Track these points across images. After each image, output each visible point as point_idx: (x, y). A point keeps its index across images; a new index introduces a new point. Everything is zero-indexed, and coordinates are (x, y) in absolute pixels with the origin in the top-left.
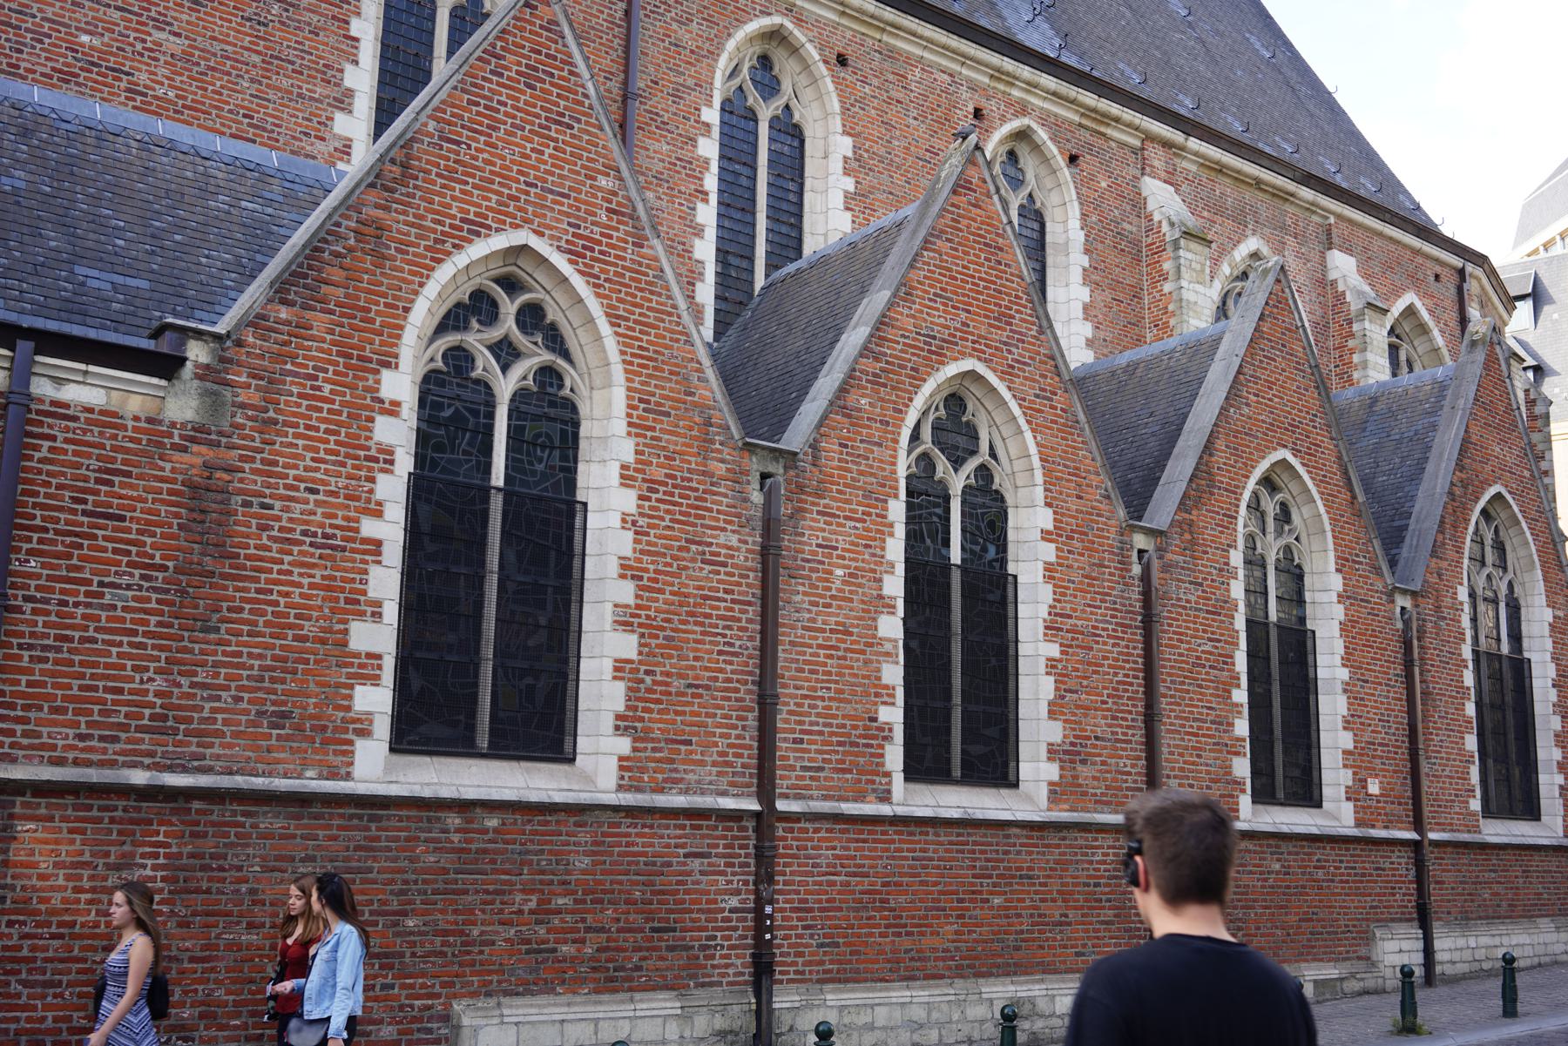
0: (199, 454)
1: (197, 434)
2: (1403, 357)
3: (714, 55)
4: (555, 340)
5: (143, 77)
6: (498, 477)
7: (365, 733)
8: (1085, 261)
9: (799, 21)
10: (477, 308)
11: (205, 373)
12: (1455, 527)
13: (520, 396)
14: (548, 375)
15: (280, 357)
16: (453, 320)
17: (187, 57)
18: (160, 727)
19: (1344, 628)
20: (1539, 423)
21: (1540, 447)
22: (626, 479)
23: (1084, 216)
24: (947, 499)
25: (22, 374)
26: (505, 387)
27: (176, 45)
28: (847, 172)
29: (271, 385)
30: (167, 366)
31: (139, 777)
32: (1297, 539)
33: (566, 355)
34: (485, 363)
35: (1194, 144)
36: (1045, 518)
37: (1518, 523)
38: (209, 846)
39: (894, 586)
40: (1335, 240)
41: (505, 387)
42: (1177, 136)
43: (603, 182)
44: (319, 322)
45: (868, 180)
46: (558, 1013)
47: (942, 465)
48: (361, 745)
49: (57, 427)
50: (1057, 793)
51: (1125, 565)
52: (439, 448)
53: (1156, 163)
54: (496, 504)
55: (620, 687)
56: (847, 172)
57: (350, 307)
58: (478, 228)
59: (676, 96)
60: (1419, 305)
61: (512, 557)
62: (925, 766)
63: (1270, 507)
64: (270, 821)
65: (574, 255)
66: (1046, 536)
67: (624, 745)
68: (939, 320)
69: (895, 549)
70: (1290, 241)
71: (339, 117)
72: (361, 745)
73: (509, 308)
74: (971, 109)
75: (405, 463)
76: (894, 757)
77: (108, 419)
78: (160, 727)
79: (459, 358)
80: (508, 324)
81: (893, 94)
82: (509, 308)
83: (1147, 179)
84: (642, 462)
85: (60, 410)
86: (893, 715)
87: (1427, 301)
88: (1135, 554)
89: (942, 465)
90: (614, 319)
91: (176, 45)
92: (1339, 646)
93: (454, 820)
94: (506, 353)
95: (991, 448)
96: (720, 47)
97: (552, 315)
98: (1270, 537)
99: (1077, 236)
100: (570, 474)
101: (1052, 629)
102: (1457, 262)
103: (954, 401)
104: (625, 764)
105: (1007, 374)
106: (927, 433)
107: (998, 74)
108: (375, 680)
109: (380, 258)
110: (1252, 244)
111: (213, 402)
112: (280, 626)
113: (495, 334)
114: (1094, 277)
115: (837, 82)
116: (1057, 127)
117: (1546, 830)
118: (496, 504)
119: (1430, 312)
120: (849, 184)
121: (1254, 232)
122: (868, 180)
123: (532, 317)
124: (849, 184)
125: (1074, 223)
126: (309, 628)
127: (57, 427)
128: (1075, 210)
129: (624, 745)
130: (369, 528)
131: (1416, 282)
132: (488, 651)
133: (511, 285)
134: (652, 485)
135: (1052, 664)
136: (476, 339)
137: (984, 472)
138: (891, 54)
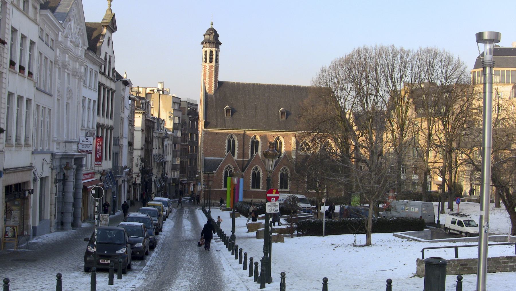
4: (231, 169)
10: (228, 168)
13: (229, 172)
14: (231, 170)
16: (226, 169)
26: (229, 172)
27: (216, 148)
34: (228, 170)
36: (262, 174)
39: (251, 179)
41: (229, 172)
47: (255, 171)
50: (262, 189)
58: (227, 165)
62: (253, 187)
69: (251, 177)
73: (229, 168)
75: (224, 176)
76: (251, 187)
79: (226, 170)
80: (229, 168)
82: (229, 168)
86: (251, 185)
89: (255, 171)
91: (216, 148)
94: (229, 170)
103: (256, 167)
107: (276, 133)
116: (282, 135)
123: (230, 168)
133: (229, 166)
136: (227, 169)
137: (258, 171)
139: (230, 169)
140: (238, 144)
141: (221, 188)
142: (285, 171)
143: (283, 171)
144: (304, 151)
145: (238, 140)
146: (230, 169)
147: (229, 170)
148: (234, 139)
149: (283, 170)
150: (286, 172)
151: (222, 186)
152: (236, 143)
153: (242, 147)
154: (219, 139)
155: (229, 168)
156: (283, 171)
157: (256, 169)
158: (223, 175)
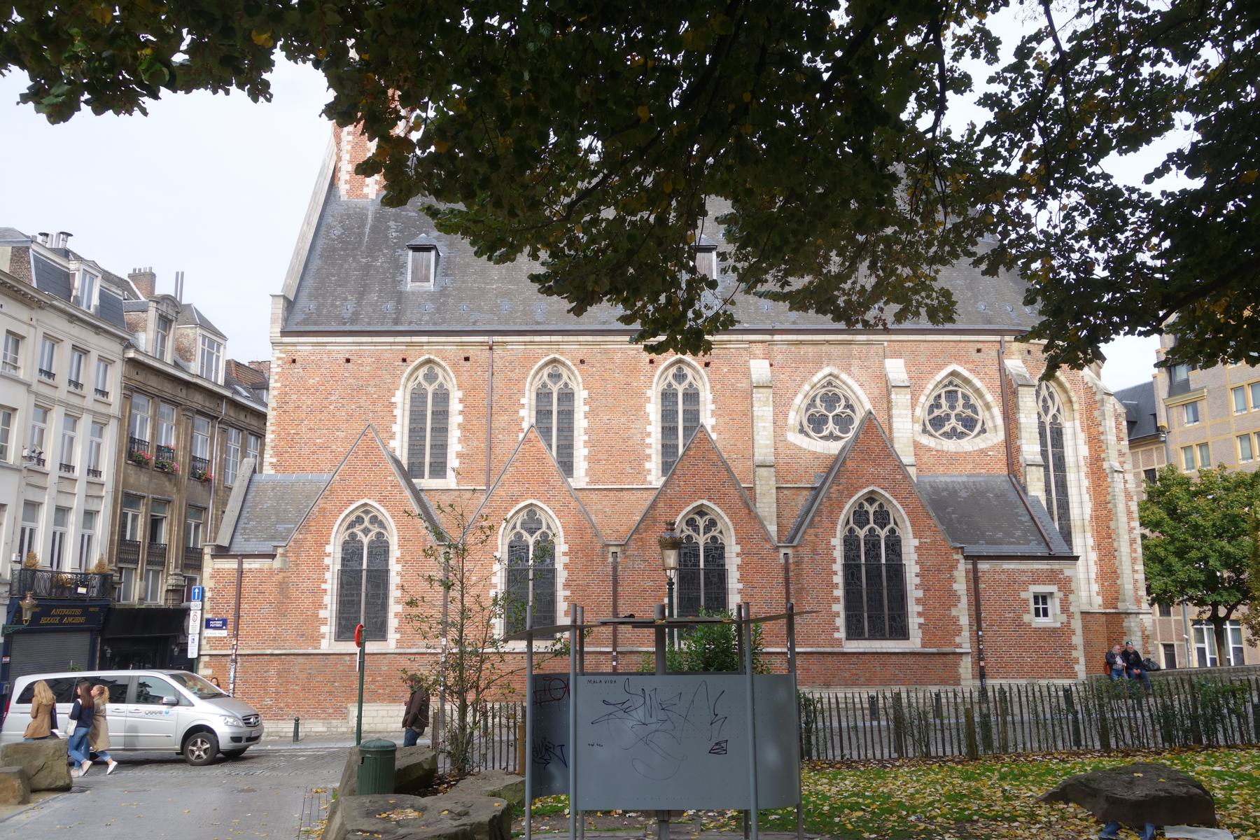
0: (282, 575)
1: (281, 570)
2: (960, 395)
3: (525, 379)
4: (382, 525)
5: (334, 447)
6: (365, 566)
7: (323, 638)
8: (713, 407)
9: (562, 354)
10: (359, 520)
11: (283, 555)
12: (831, 512)
13: (371, 542)
14: (380, 535)
15: (300, 548)
16: (351, 525)
17: (346, 437)
18: (275, 639)
19: (740, 567)
20: (1098, 405)
21: (1099, 419)
22: (398, 561)
23: (712, 388)
24: (528, 546)
25: (241, 564)
26: (366, 541)
28: (585, 404)
29: (298, 555)
30: (273, 556)
31: (268, 652)
32: (721, 532)
33: (385, 528)
34: (360, 535)
35: (777, 337)
37: (891, 502)
38: (286, 666)
40: (888, 353)
41: (366, 541)
42: (768, 337)
43: (389, 478)
44: (309, 537)
45: (594, 405)
46: (376, 708)
48: (322, 640)
49: (249, 574)
51: (604, 558)
52: (348, 561)
53: (757, 352)
54: (364, 573)
55: (397, 620)
56: (585, 404)
57: (318, 531)
58: (351, 502)
59: (510, 398)
60: (959, 369)
61: (369, 586)
63: (701, 523)
64: (301, 660)
65: (380, 501)
66: (565, 554)
67: (398, 636)
68: (516, 489)
70: (856, 362)
71: (391, 442)
72: (322, 640)
73: (367, 519)
74: (648, 360)
77: (260, 571)
78: (275, 639)
79: (353, 536)
80: (366, 523)
81: (608, 367)
82: (367, 519)
83: (752, 361)
84: (403, 556)
85: (250, 570)
87: (967, 366)
88: (610, 555)
89: (526, 535)
90: (393, 517)
92: (737, 575)
93: (347, 658)
95: (548, 525)
96: (527, 375)
97: (380, 517)
98: (702, 534)
99: (710, 397)
100: (387, 561)
101: (566, 586)
102: (998, 338)
104: (398, 641)
105: (547, 501)
106: (518, 525)
108: (326, 624)
109: (324, 517)
110: (827, 370)
111: (284, 562)
112: (302, 613)
113: (362, 527)
114: (719, 412)
115: (580, 371)
117: (914, 643)
118: (364, 573)
119: (971, 371)
120: (587, 408)
121: (828, 365)
122: (594, 405)
123: (374, 520)
124: (587, 408)
125: (708, 392)
126: (309, 613)
127: (249, 574)
128: (708, 386)
129: (398, 636)
130: (323, 586)
131: (958, 358)
132: (362, 613)
133: (367, 512)
134: (406, 562)
135: (566, 598)
136: (357, 530)
137: (545, 535)
138: (606, 351)
139: (375, 529)
140: (460, 407)
141: (316, 638)
142: (708, 529)
143: (696, 529)
144: (825, 433)
145: (460, 388)
146: (375, 529)
147: (372, 535)
148: (441, 385)
149: (691, 523)
150: (714, 539)
151: (324, 629)
152: (455, 406)
153: (484, 421)
154: (360, 388)
155: (366, 523)
156: (696, 529)
157: (532, 523)
158: (327, 561)
